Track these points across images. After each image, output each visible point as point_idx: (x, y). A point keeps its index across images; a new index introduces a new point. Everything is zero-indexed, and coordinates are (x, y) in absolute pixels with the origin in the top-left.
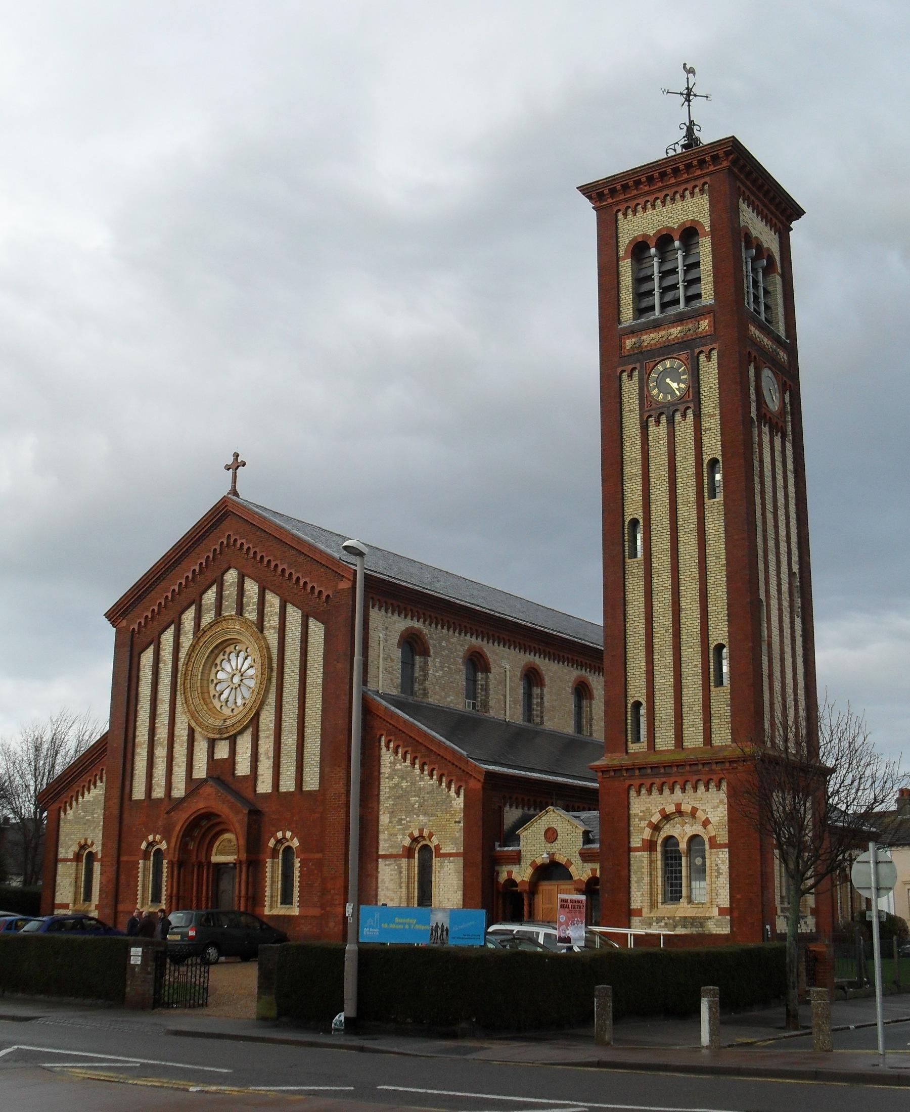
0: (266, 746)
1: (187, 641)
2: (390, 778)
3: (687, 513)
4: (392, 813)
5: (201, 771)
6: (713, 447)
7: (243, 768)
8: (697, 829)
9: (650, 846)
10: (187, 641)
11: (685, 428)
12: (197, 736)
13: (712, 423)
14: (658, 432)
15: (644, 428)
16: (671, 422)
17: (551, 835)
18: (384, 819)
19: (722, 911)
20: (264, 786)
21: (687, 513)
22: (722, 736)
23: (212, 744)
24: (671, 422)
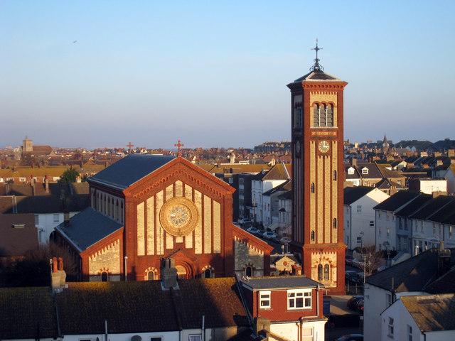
0: (198, 239)
1: (160, 204)
2: (238, 248)
3: (327, 183)
4: (240, 259)
5: (170, 245)
6: (335, 167)
7: (189, 245)
8: (327, 262)
9: (315, 267)
10: (160, 204)
11: (328, 160)
12: (167, 235)
13: (335, 161)
14: (320, 160)
15: (316, 158)
16: (324, 158)
17: (285, 264)
18: (236, 260)
19: (335, 282)
20: (198, 251)
21: (327, 183)
22: (335, 240)
23: (174, 239)
24: (324, 158)
